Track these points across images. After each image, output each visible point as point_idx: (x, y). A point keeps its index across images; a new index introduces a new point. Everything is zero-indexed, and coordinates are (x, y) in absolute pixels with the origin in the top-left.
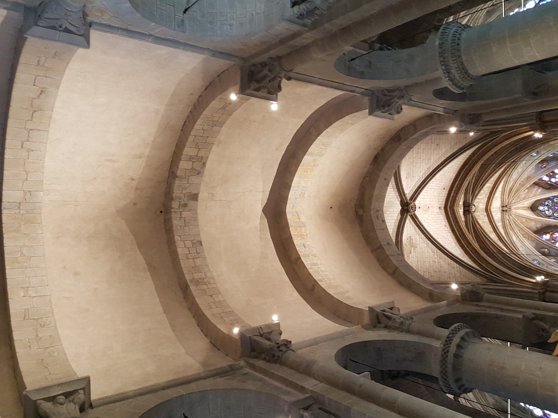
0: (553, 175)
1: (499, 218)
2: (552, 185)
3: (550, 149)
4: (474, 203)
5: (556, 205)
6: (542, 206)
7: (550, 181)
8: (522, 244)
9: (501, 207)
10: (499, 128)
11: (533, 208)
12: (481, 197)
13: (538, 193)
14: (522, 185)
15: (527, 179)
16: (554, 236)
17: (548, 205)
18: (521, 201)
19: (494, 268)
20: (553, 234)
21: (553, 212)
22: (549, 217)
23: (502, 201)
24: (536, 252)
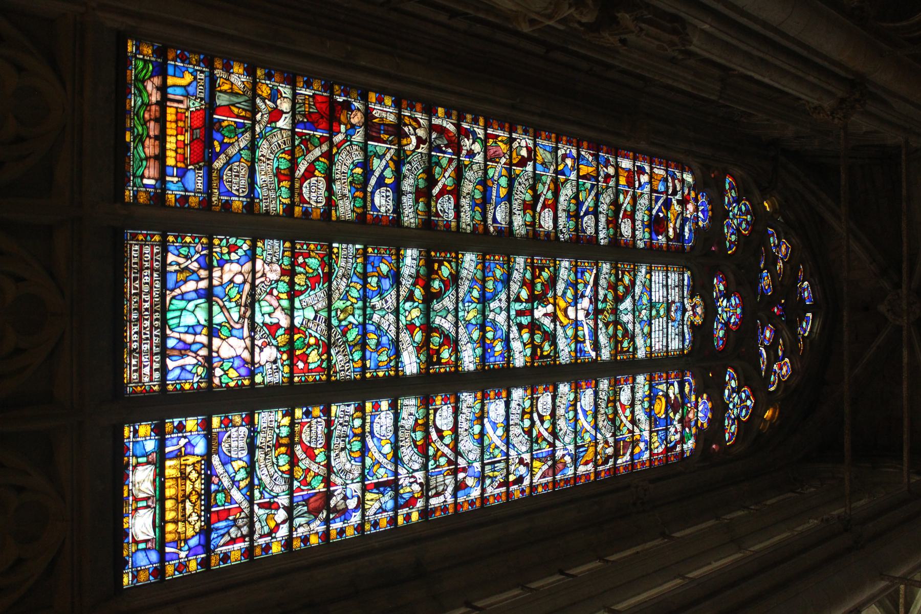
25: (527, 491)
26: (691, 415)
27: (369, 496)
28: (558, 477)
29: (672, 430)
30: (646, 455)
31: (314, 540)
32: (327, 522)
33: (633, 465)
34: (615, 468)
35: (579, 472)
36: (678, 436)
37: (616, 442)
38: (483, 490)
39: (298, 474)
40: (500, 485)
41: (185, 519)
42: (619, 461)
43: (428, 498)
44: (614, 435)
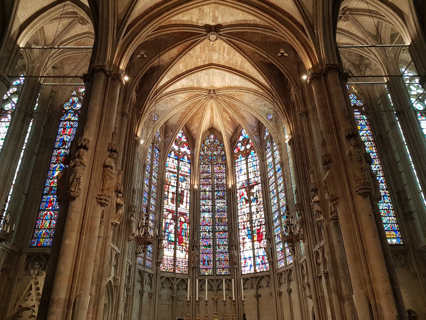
0: (245, 144)
1: (202, 84)
2: (235, 143)
3: (274, 130)
4: (219, 40)
5: (215, 147)
6: (214, 137)
7: (239, 142)
8: (174, 107)
9: (214, 88)
10: (317, 33)
11: (212, 130)
12: (225, 56)
13: (227, 130)
14: (236, 111)
15: (242, 117)
16: (185, 145)
17: (215, 141)
18: (219, 111)
19: (137, 32)
20: (187, 145)
21: (208, 146)
22: (203, 142)
23: (220, 88)
24: (166, 118)
25: (380, 165)
26: (359, 117)
27: (385, 202)
28: (377, 158)
29: (362, 123)
30: (369, 131)
31: (393, 212)
32: (390, 210)
33: (371, 136)
34: (373, 141)
35: (375, 152)
36: (364, 121)
37: (368, 141)
38: (381, 176)
39: (384, 215)
40: (380, 172)
41: (393, 234)
42: (371, 140)
43: (384, 189)
44: (366, 142)
